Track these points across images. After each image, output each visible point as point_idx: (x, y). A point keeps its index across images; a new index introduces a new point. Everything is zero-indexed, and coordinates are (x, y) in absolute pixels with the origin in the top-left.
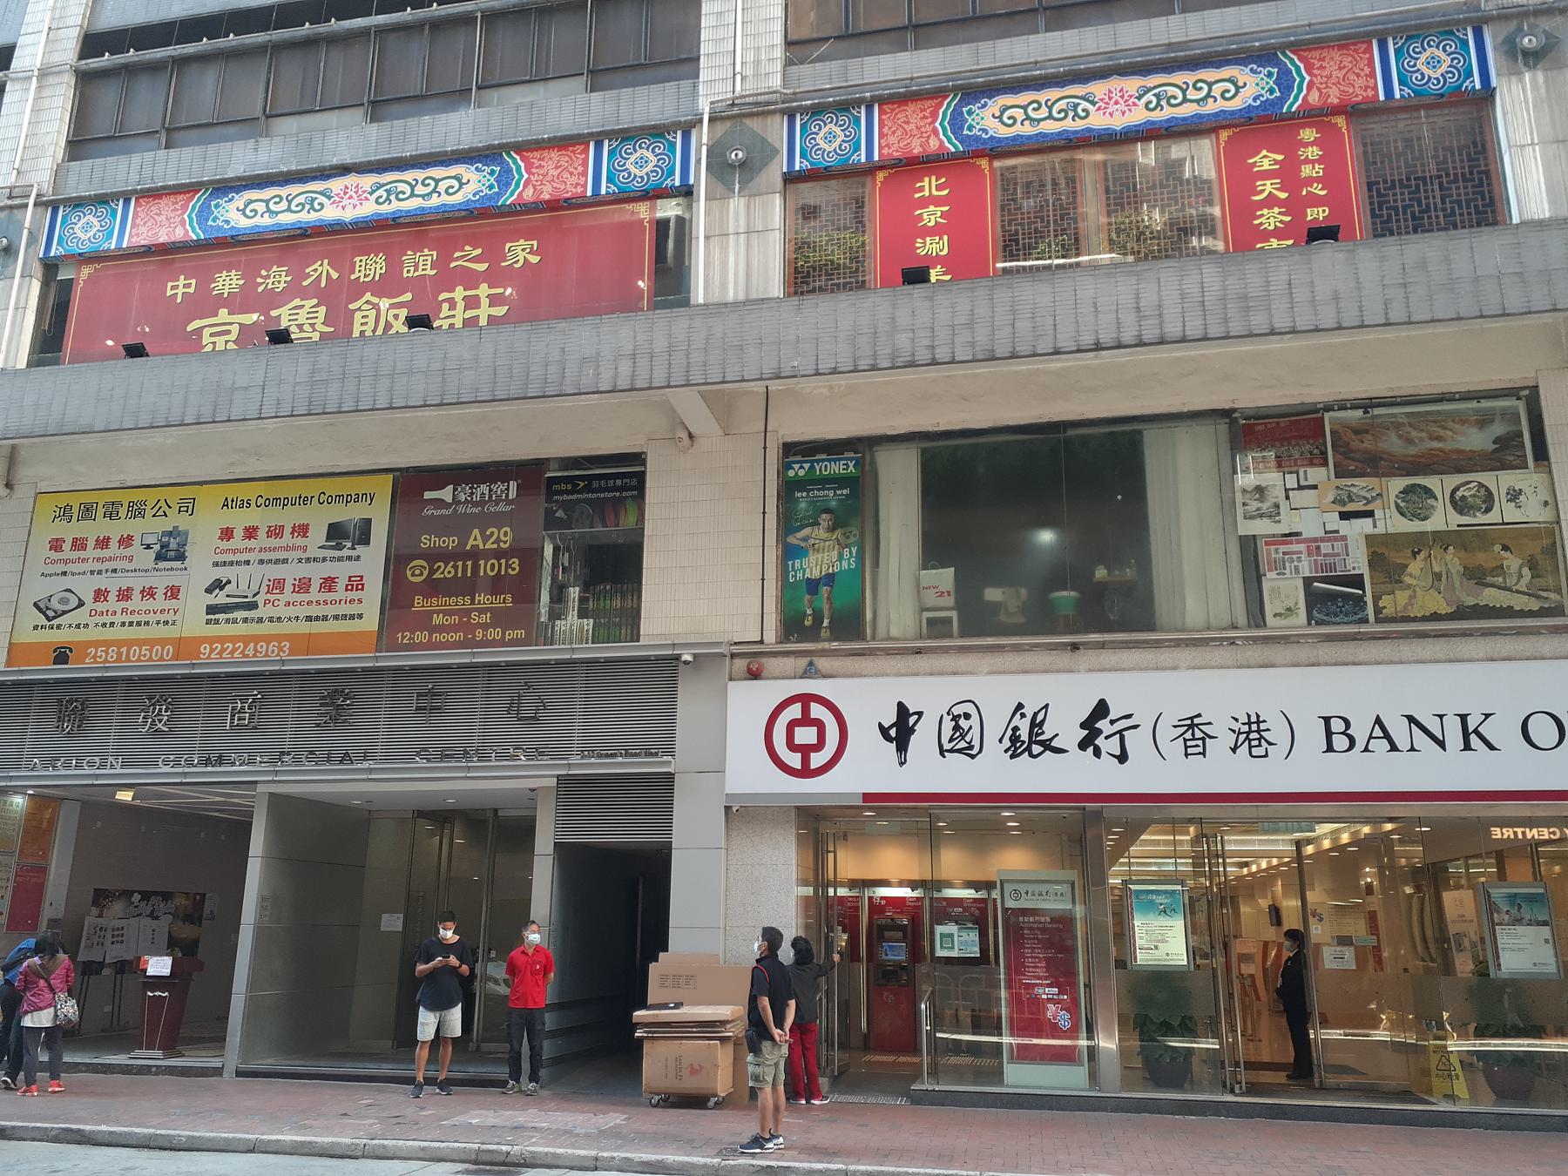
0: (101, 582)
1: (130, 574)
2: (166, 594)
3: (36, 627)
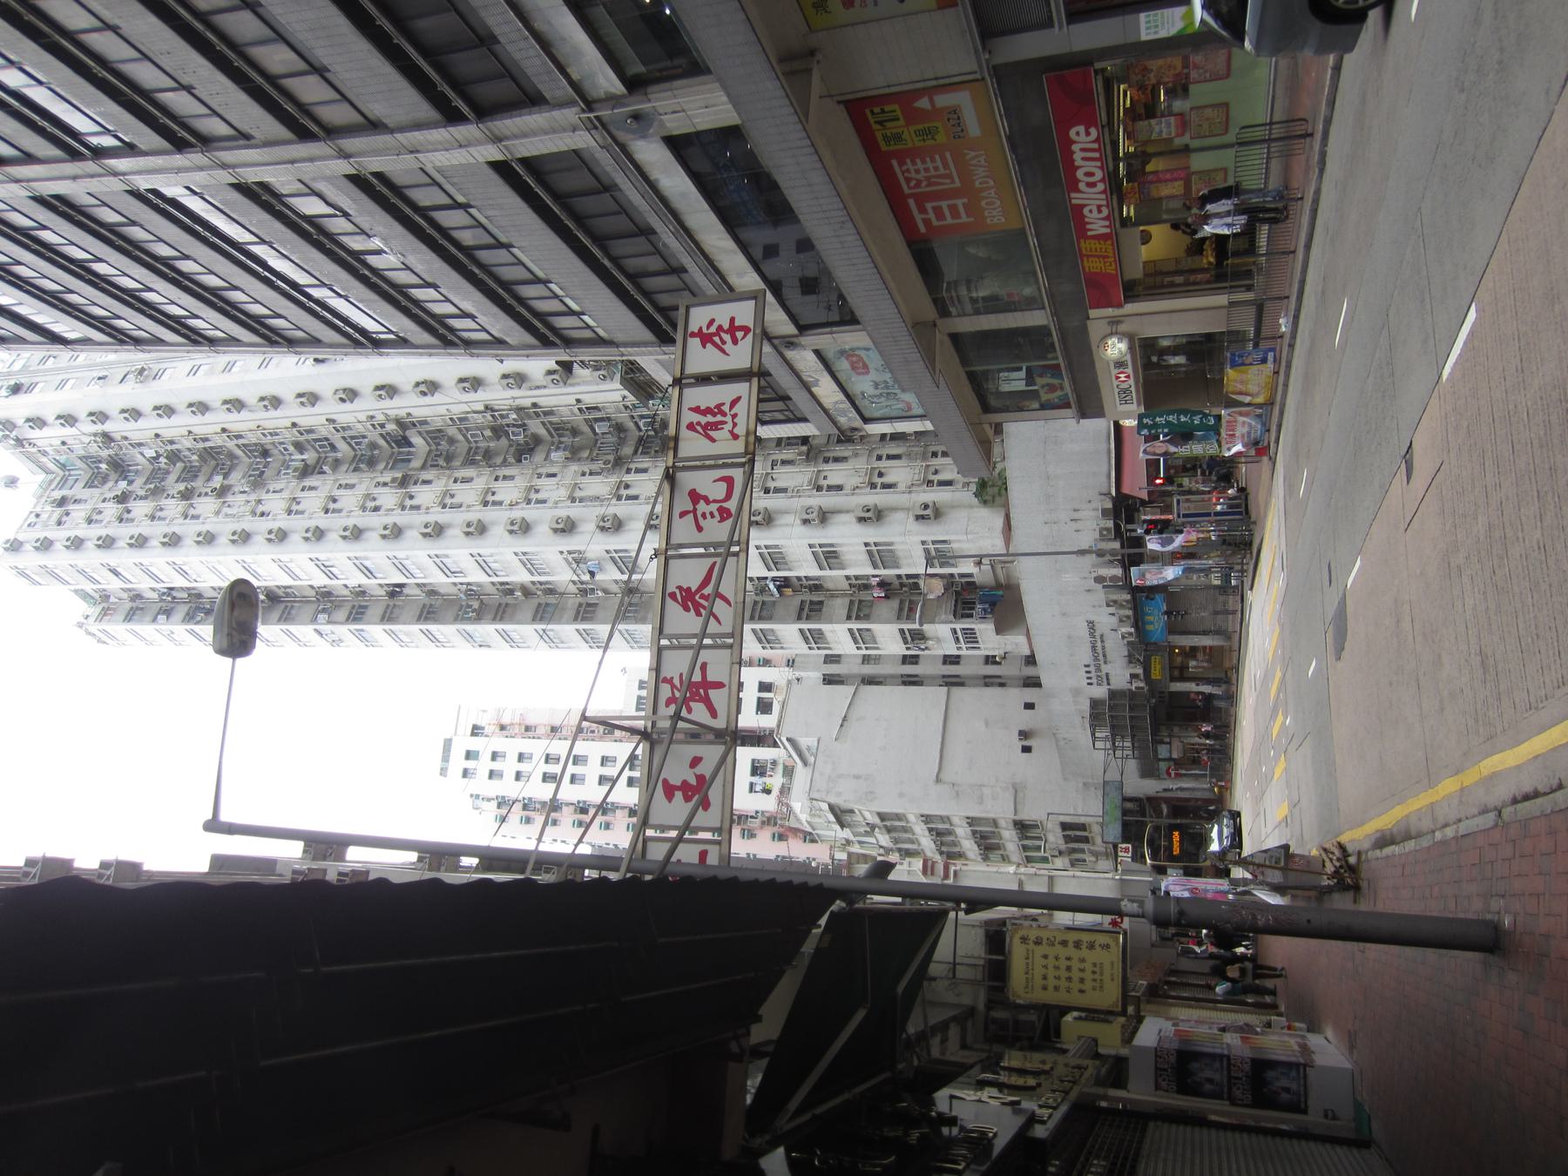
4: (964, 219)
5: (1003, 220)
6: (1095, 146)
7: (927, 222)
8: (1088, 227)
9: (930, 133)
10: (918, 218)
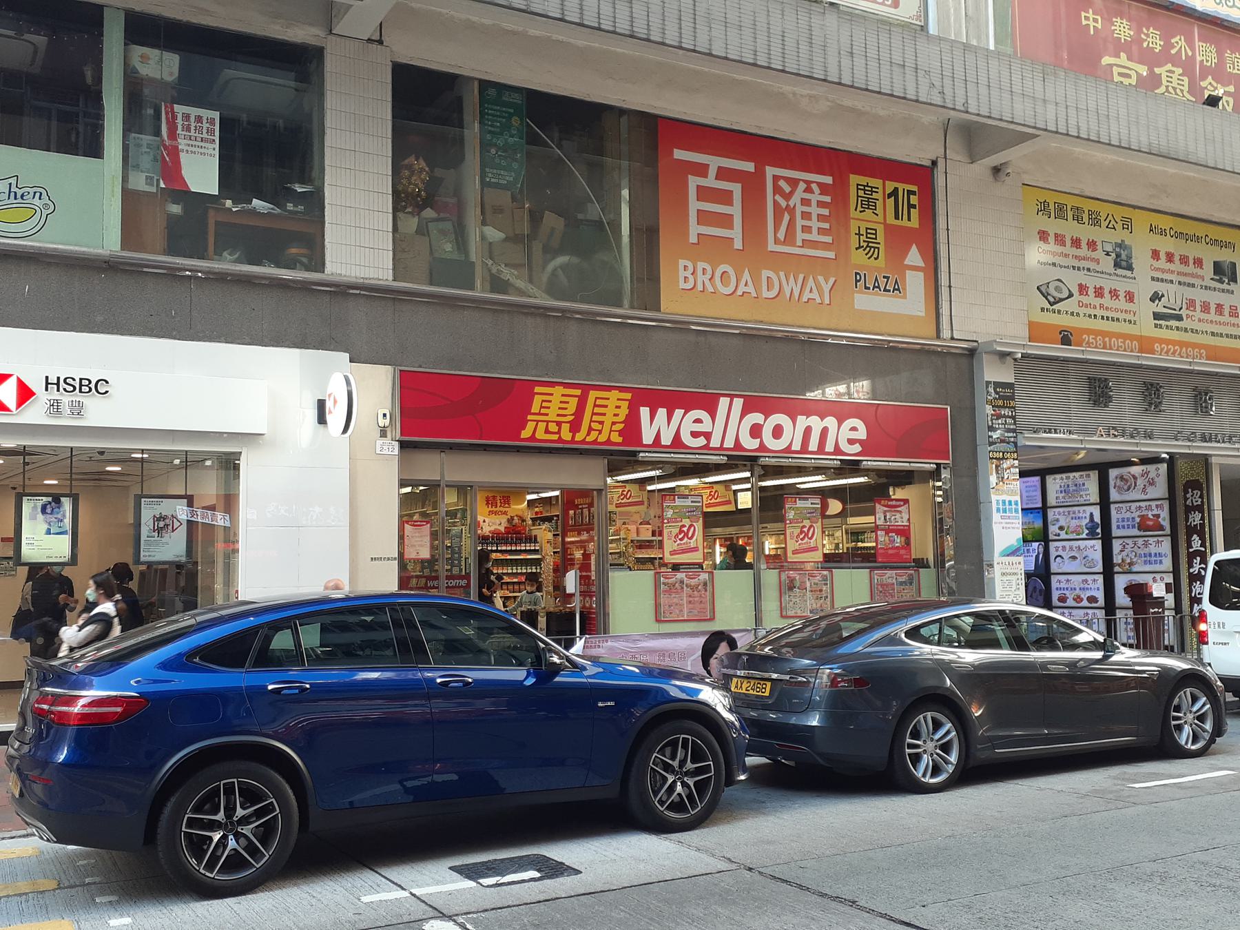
0: (1082, 278)
1: (1099, 275)
2: (1126, 297)
3: (1042, 309)
4: (695, 230)
5: (682, 285)
6: (830, 447)
7: (702, 170)
8: (662, 413)
9: (869, 246)
10: (714, 162)
